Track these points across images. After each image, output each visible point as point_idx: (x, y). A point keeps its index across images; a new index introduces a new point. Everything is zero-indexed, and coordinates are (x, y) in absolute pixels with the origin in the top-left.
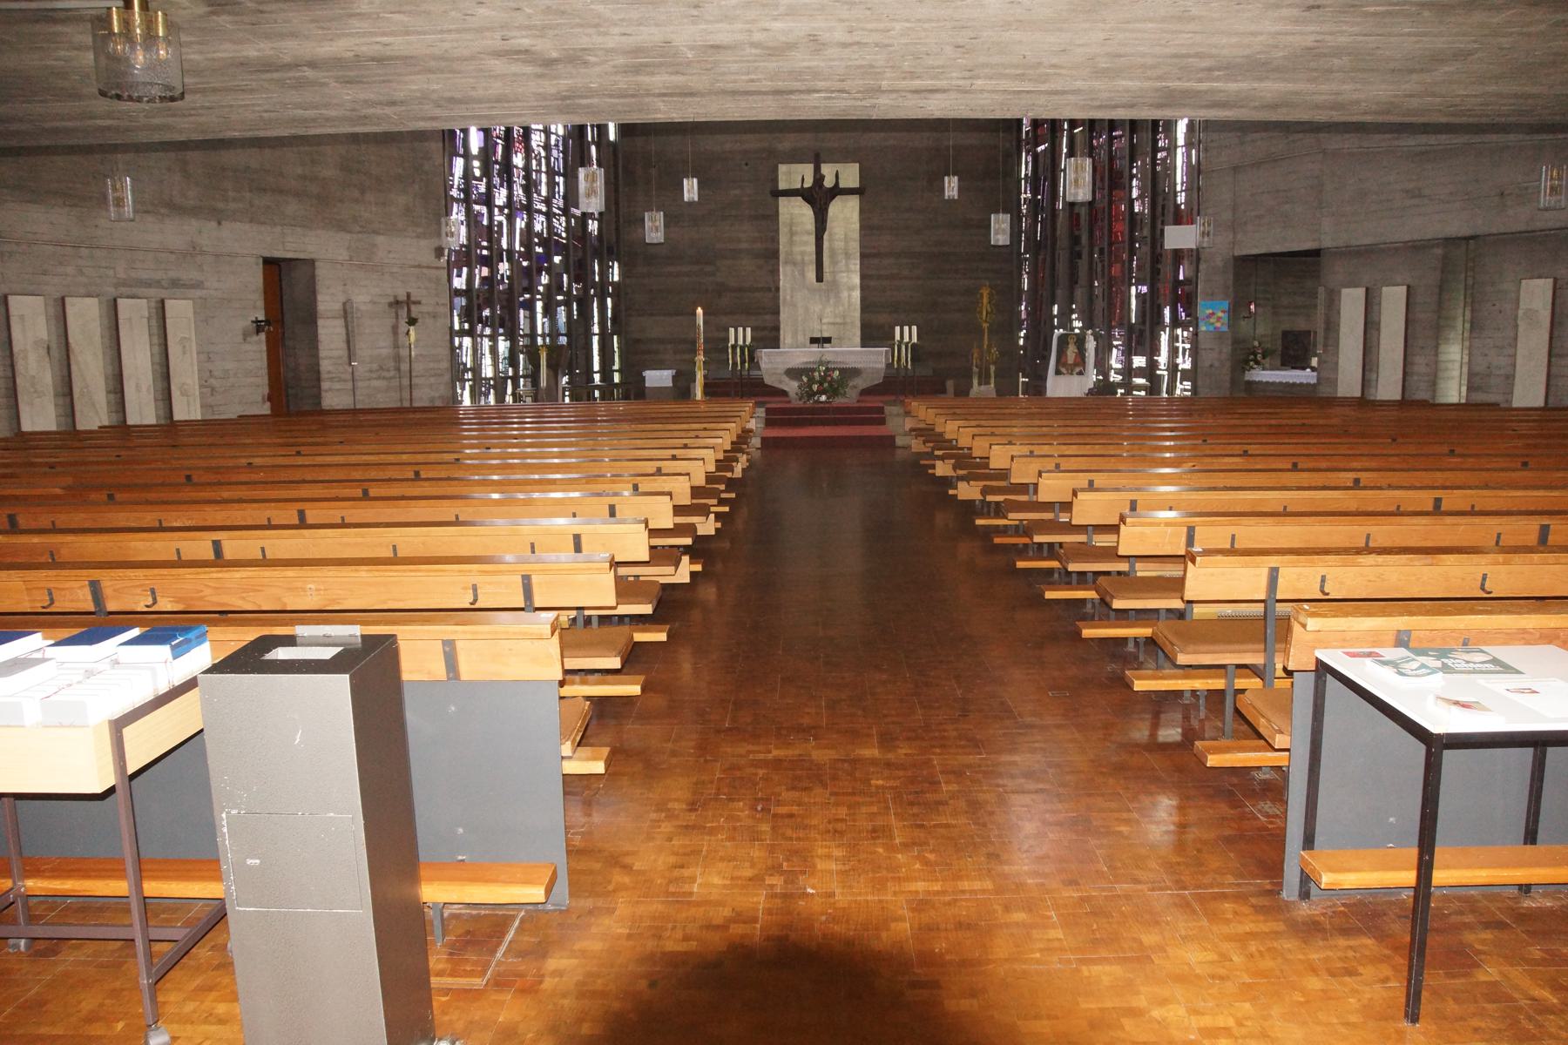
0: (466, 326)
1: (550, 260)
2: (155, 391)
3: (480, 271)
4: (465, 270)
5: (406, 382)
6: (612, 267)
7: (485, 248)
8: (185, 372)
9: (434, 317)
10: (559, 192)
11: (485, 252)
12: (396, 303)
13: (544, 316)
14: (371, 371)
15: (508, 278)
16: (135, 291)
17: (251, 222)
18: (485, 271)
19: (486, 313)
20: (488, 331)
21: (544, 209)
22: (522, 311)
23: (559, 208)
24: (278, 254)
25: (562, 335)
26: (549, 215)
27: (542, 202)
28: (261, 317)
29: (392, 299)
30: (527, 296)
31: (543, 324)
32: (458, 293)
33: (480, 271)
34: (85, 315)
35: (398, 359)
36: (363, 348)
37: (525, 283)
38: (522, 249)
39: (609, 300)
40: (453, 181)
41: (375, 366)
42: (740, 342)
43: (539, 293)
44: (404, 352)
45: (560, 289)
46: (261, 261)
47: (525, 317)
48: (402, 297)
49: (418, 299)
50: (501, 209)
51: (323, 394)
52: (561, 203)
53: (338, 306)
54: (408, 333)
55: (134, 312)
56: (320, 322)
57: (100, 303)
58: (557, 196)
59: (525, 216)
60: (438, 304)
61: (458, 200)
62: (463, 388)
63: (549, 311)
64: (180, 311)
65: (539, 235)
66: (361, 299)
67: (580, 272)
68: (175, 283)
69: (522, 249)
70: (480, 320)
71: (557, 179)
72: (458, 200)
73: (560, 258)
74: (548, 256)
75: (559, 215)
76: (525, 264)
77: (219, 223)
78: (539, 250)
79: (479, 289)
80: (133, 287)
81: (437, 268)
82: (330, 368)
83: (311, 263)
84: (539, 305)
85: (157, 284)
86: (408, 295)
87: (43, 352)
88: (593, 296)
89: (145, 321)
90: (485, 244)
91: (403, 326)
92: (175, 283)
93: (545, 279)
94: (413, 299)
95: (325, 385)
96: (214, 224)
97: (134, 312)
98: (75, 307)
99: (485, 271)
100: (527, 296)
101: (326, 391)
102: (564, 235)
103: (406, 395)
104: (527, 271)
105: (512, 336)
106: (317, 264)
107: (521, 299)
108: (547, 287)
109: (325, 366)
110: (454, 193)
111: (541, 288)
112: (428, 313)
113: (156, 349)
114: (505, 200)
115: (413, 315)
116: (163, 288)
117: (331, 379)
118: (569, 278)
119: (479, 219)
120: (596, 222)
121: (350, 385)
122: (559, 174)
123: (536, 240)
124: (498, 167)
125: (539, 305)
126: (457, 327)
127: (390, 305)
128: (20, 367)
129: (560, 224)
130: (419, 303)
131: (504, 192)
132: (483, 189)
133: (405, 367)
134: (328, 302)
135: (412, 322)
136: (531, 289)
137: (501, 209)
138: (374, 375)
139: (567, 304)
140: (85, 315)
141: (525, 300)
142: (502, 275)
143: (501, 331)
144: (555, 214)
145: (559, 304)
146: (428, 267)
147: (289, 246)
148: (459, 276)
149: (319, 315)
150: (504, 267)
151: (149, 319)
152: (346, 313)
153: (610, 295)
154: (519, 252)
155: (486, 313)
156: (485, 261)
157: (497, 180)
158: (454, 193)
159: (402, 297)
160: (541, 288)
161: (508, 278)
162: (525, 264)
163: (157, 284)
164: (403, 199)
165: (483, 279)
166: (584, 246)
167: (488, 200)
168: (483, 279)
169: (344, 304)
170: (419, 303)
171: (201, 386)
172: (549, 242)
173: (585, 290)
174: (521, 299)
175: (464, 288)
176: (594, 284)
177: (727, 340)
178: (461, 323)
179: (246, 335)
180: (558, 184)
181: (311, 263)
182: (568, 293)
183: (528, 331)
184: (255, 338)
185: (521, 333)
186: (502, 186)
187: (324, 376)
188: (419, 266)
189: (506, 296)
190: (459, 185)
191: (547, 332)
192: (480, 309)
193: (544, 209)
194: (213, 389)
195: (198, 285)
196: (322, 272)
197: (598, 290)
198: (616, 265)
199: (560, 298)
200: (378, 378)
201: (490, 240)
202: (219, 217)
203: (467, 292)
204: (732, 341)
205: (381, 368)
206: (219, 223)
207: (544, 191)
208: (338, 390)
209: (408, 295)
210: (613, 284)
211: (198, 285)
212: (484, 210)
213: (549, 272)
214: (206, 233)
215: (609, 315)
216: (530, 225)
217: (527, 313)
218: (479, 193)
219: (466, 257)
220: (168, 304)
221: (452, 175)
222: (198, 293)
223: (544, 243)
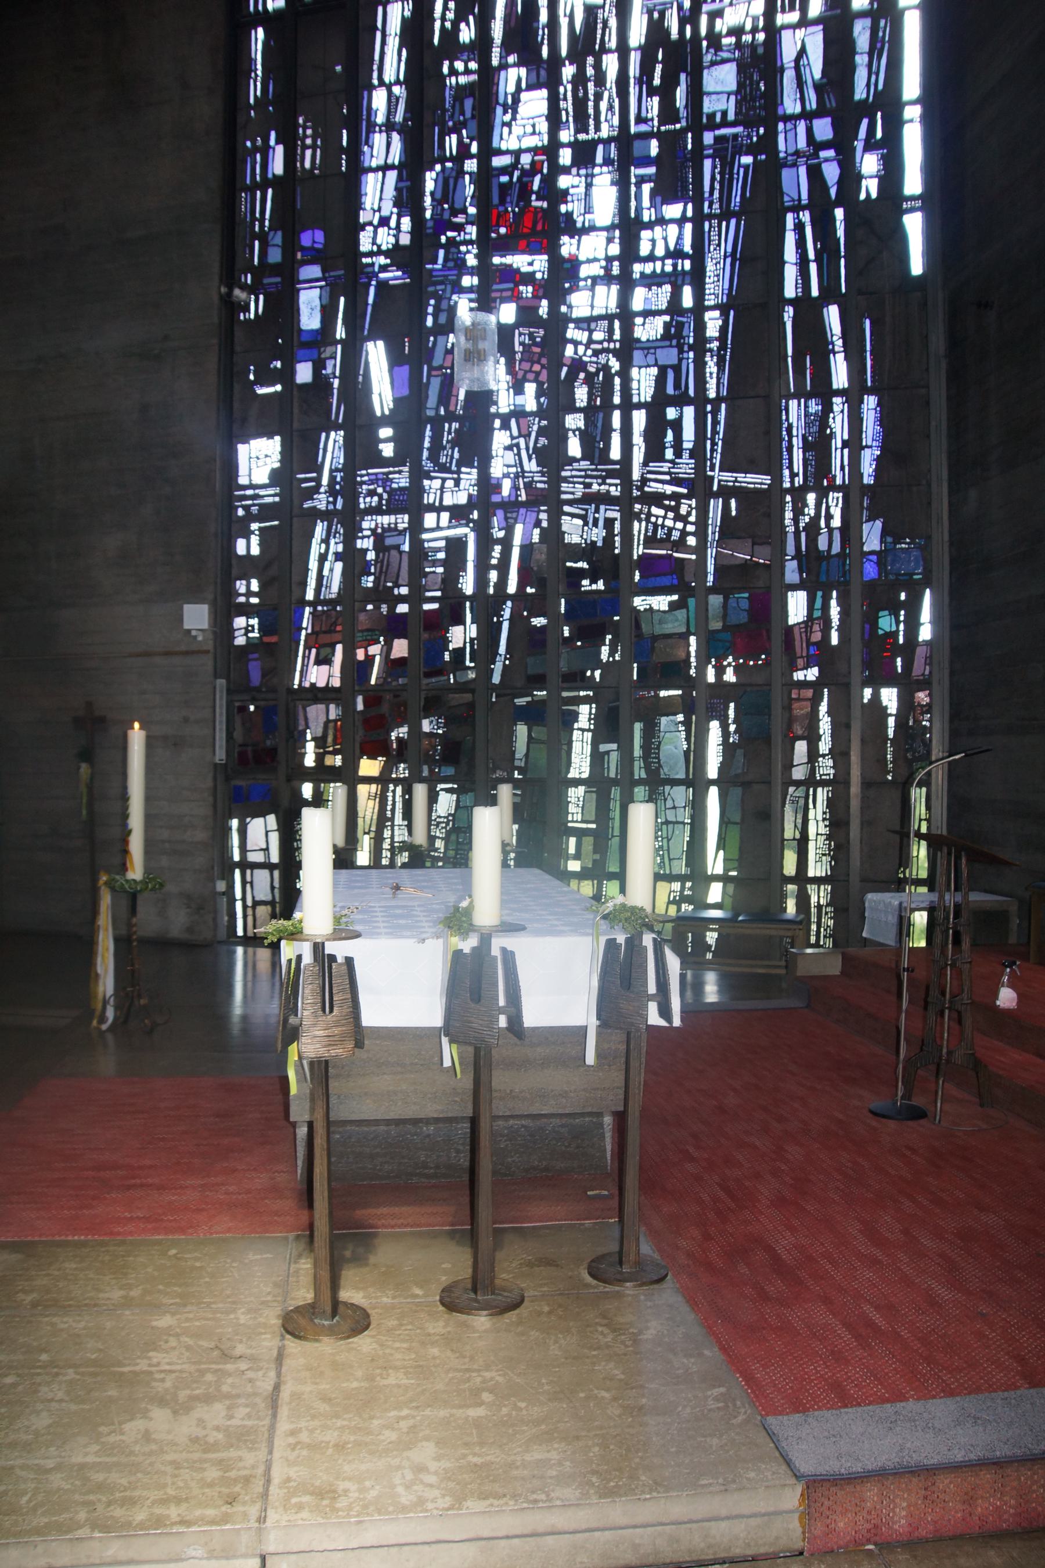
7: (402, 599)
9: (175, 745)
11: (403, 608)
18: (400, 648)
23: (676, 481)
25: (675, 783)
27: (611, 474)
40: (318, 480)
58: (669, 454)
59: (543, 516)
60: (186, 720)
61: (326, 515)
75: (676, 496)
90: (404, 591)
107: (521, 701)
122: (681, 400)
124: (455, 425)
148: (324, 660)
150: (459, 636)
174: (521, 701)
180: (677, 425)
193: (615, 492)
215: (891, 733)
218: (392, 493)
221: (319, 470)
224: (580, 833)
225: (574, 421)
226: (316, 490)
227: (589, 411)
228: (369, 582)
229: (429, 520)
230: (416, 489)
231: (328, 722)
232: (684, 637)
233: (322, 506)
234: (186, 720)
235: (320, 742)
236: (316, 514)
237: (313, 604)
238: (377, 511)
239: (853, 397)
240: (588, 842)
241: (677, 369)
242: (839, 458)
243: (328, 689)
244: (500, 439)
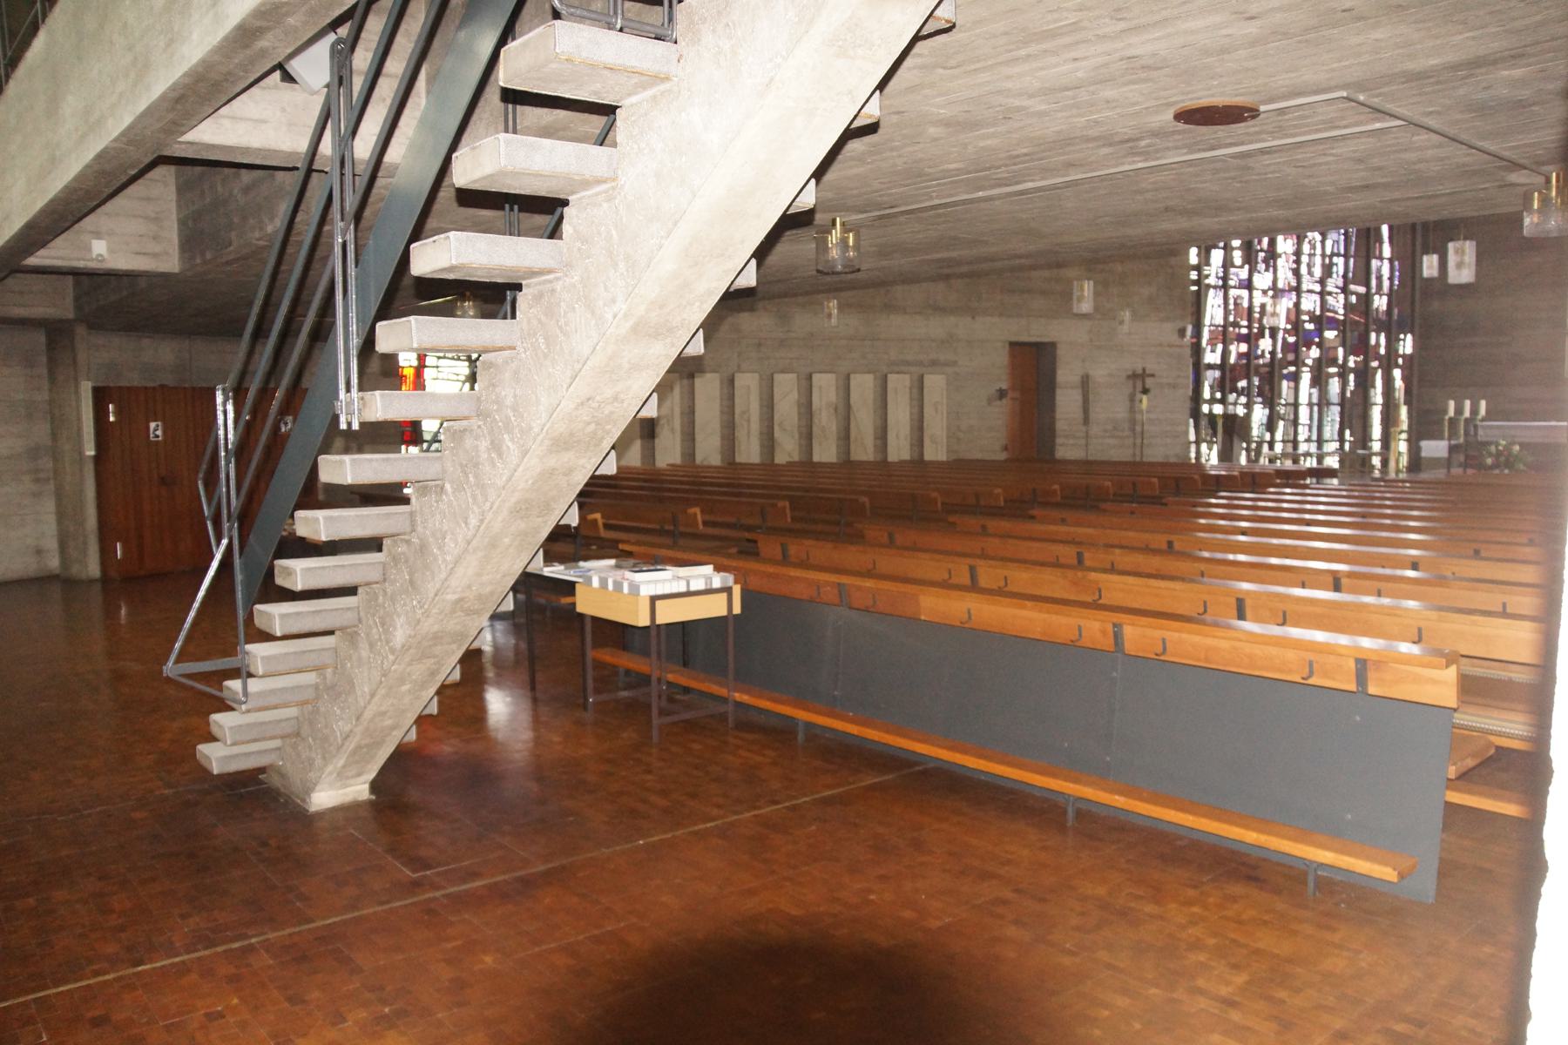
0: (1218, 395)
1: (1321, 336)
2: (912, 439)
3: (1238, 346)
4: (1220, 347)
5: (1139, 441)
6: (1404, 340)
8: (936, 426)
9: (1174, 387)
10: (1337, 272)
12: (1134, 376)
13: (1313, 385)
14: (1106, 431)
15: (1270, 353)
16: (903, 368)
17: (1001, 315)
18: (1244, 347)
19: (1242, 384)
20: (1243, 400)
21: (1317, 288)
22: (1285, 384)
23: (1337, 287)
24: (1024, 338)
25: (1334, 404)
26: (1323, 294)
27: (1317, 282)
28: (1004, 386)
29: (1130, 373)
30: (1292, 369)
31: (1310, 395)
32: (1211, 367)
33: (1238, 346)
34: (863, 385)
35: (1133, 422)
36: (1097, 412)
37: (1291, 357)
38: (1289, 327)
39: (1397, 373)
41: (1109, 427)
42: (1467, 414)
43: (1306, 365)
44: (1138, 417)
45: (1334, 362)
46: (1007, 346)
47: (1288, 387)
48: (1140, 371)
49: (1151, 372)
50: (1265, 292)
51: (1057, 447)
52: (1340, 282)
53: (1076, 379)
54: (1141, 401)
55: (899, 384)
56: (1059, 392)
57: (875, 379)
58: (1334, 276)
61: (1215, 287)
62: (1210, 449)
63: (1319, 380)
64: (935, 383)
65: (1311, 314)
66: (1099, 373)
67: (1360, 346)
68: (934, 363)
69: (1289, 327)
70: (1234, 389)
71: (1335, 259)
72: (1215, 287)
73: (1336, 333)
74: (1319, 331)
75: (1336, 293)
76: (1292, 339)
77: (973, 318)
78: (1310, 326)
79: (1234, 365)
80: (899, 366)
81: (1181, 346)
82: (1066, 427)
83: (1052, 346)
84: (1306, 378)
85: (921, 364)
86: (1144, 370)
87: (832, 411)
88: (1376, 369)
89: (908, 390)
91: (1139, 396)
92: (934, 363)
93: (1315, 352)
94: (1147, 372)
95: (1059, 441)
96: (969, 319)
97: (899, 384)
98: (856, 380)
99: (1244, 347)
100: (1292, 369)
101: (1061, 445)
102: (1341, 311)
103: (1138, 452)
104: (1295, 348)
105: (1270, 402)
106: (1058, 346)
107: (1285, 371)
108: (1318, 361)
109: (1060, 425)
110: (1212, 281)
111: (1309, 362)
112: (1169, 384)
113: (916, 410)
114: (1271, 284)
115: (1147, 386)
116: (924, 366)
117: (1066, 437)
118: (1345, 352)
119: (1239, 301)
120: (1385, 299)
121: (1083, 442)
122: (1338, 255)
123: (1306, 318)
125: (1306, 378)
126: (1207, 394)
127: (1129, 377)
128: (816, 420)
129: (1337, 303)
130: (1153, 375)
131: (1269, 276)
132: (1244, 274)
133: (1138, 428)
134: (1067, 374)
135: (1145, 391)
136: (1298, 362)
137: (1265, 292)
138: (1107, 434)
139: (1343, 375)
140: (863, 385)
141: (1290, 373)
142: (1263, 351)
143: (1259, 400)
144: (1330, 294)
145: (1332, 375)
146: (1170, 346)
147: (1036, 331)
149: (1057, 385)
150: (1265, 344)
151: (911, 388)
152: (1085, 383)
153: (1397, 366)
154: (1286, 331)
155: (1242, 384)
156: (1241, 338)
157: (1261, 266)
158: (1212, 281)
159: (1140, 371)
160: (1309, 362)
161: (1270, 353)
162: (1292, 339)
163: (921, 364)
164: (1146, 291)
165: (1240, 355)
166: (1367, 319)
167: (1248, 285)
168: (1240, 355)
169: (1082, 377)
170: (1153, 375)
171: (948, 437)
172: (1321, 321)
173: (1366, 362)
174: (1285, 371)
175: (1219, 362)
176: (1378, 357)
177: (1445, 411)
178: (1212, 394)
179: (990, 401)
180: (1336, 265)
181: (1052, 346)
182: (1344, 366)
183: (1291, 400)
184: (999, 403)
185: (1283, 402)
186: (1267, 270)
187: (1058, 432)
188: (1161, 345)
189: (1267, 369)
190: (1217, 273)
191: (1315, 400)
192: (1235, 380)
194: (959, 439)
195: (955, 363)
196: (1061, 352)
197: (1384, 361)
198: (1409, 337)
199: (1333, 370)
200: (1113, 437)
201: (1250, 319)
202: (973, 313)
203: (1223, 366)
204: (1451, 413)
205: (1115, 428)
206: (973, 318)
207: (1318, 271)
208: (1072, 445)
209: (1144, 370)
210: (1404, 356)
211: (955, 363)
212: (1245, 293)
213: (1319, 345)
214: (961, 326)
216: (1297, 305)
217: (1292, 384)
218: (1240, 280)
219: (1224, 335)
220: (926, 377)
222: (949, 370)
223: (1313, 318)
224: (1304, 425)
225: (1305, 259)
226: (1209, 275)
227: (1310, 255)
228: (1231, 318)
229: (1255, 293)
230: (1250, 280)
231: (1215, 379)
232: (1336, 348)
233: (1213, 283)
234: (1179, 376)
235: (1211, 387)
236: (1209, 286)
237: (1210, 326)
238: (1235, 287)
239: (1391, 260)
240: (1307, 428)
241: (1338, 242)
242: (1386, 284)
243: (1215, 365)
244: (1280, 262)
